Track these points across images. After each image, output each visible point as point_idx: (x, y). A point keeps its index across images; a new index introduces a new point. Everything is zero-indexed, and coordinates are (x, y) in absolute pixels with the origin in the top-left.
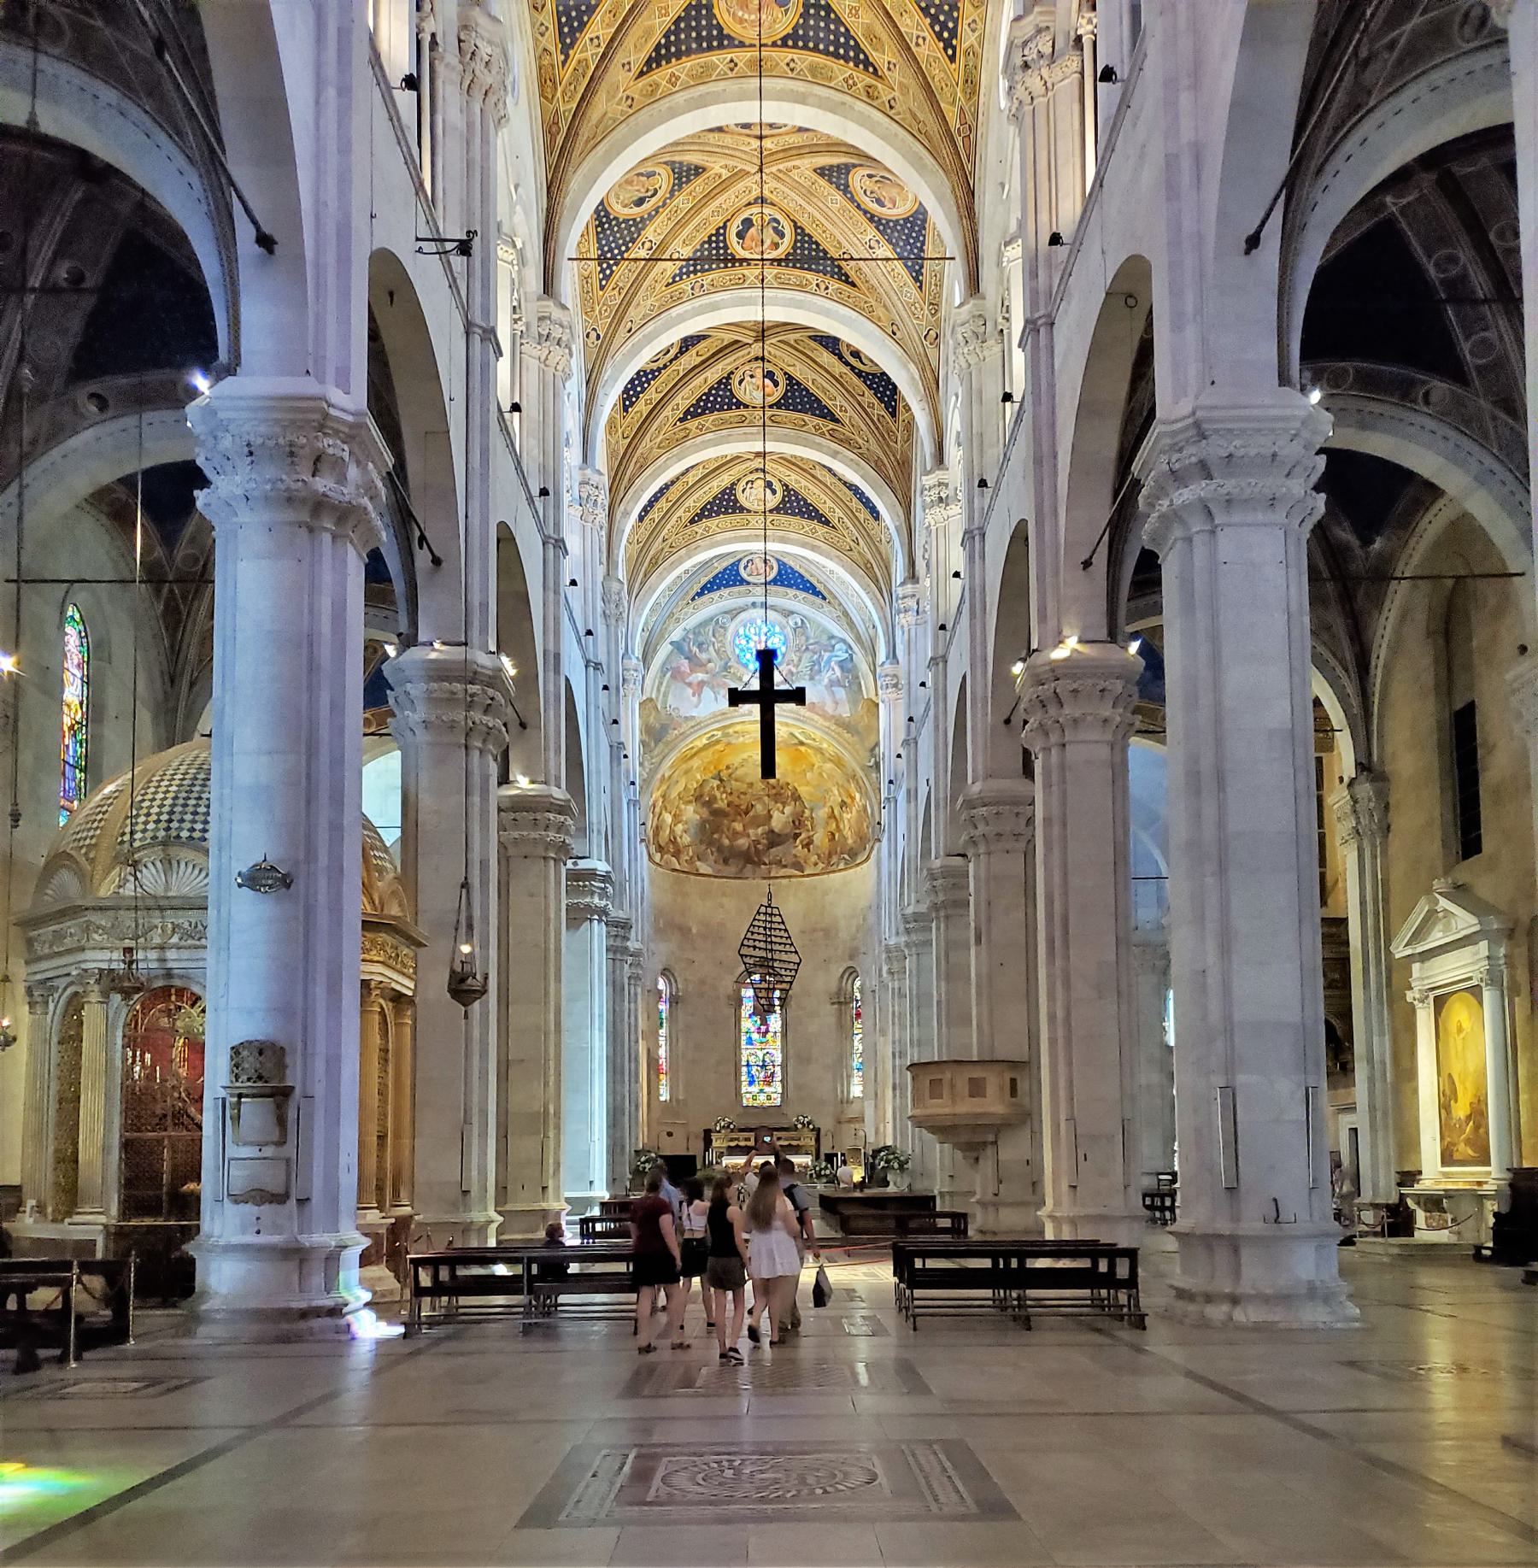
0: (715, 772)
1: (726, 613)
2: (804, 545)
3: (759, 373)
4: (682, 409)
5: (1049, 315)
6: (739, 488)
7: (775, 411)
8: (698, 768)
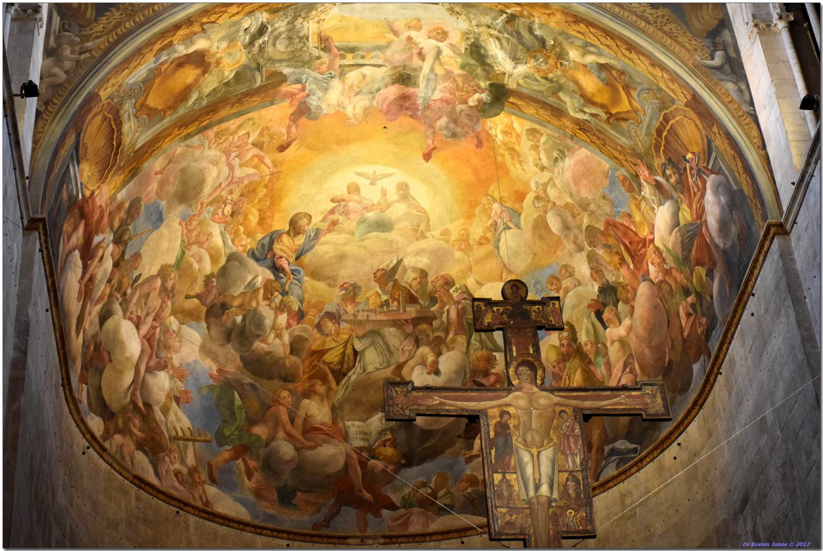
8: (219, 201)
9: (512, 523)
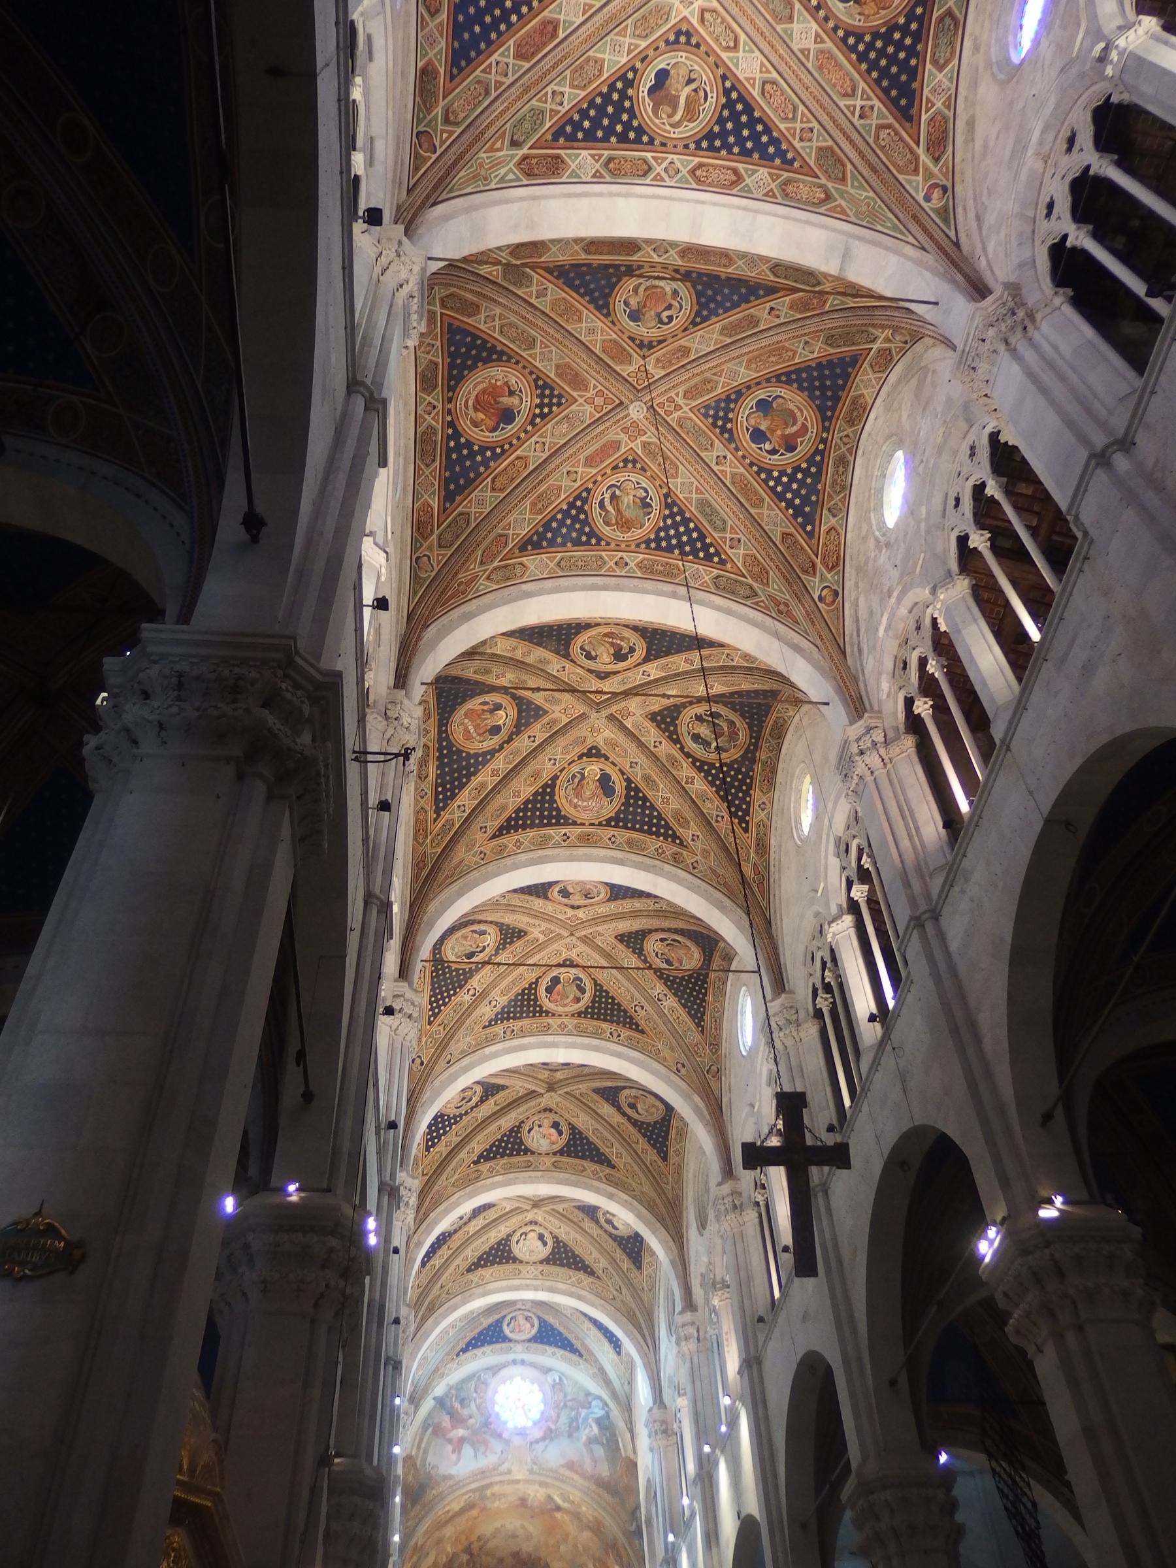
0: (466, 1543)
1: (487, 1369)
2: (571, 1295)
3: (547, 1123)
4: (477, 1151)
5: (933, 911)
6: (514, 1239)
7: (558, 1158)
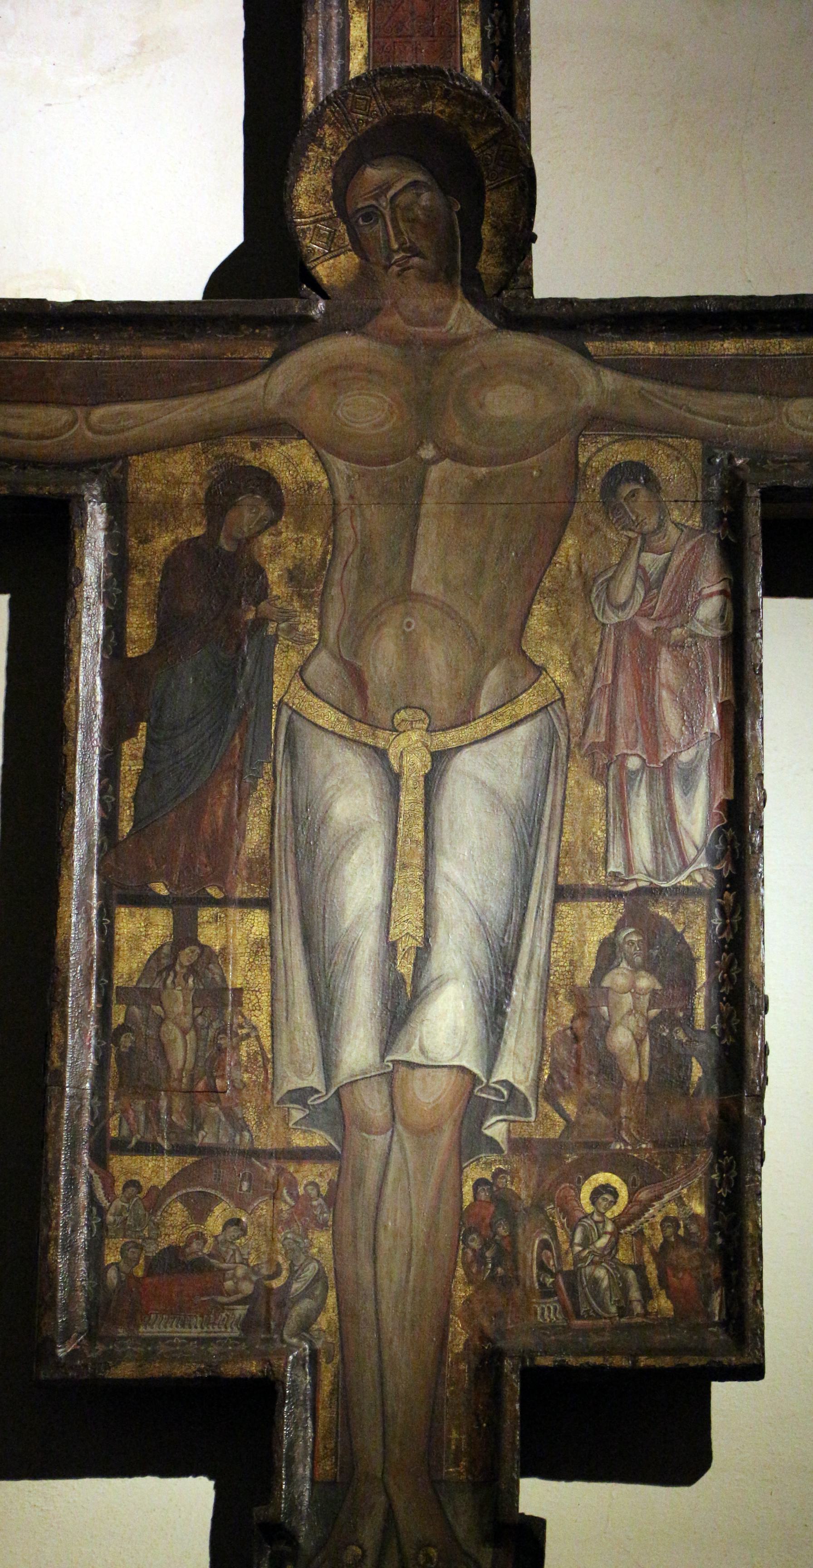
9: (200, 1266)
